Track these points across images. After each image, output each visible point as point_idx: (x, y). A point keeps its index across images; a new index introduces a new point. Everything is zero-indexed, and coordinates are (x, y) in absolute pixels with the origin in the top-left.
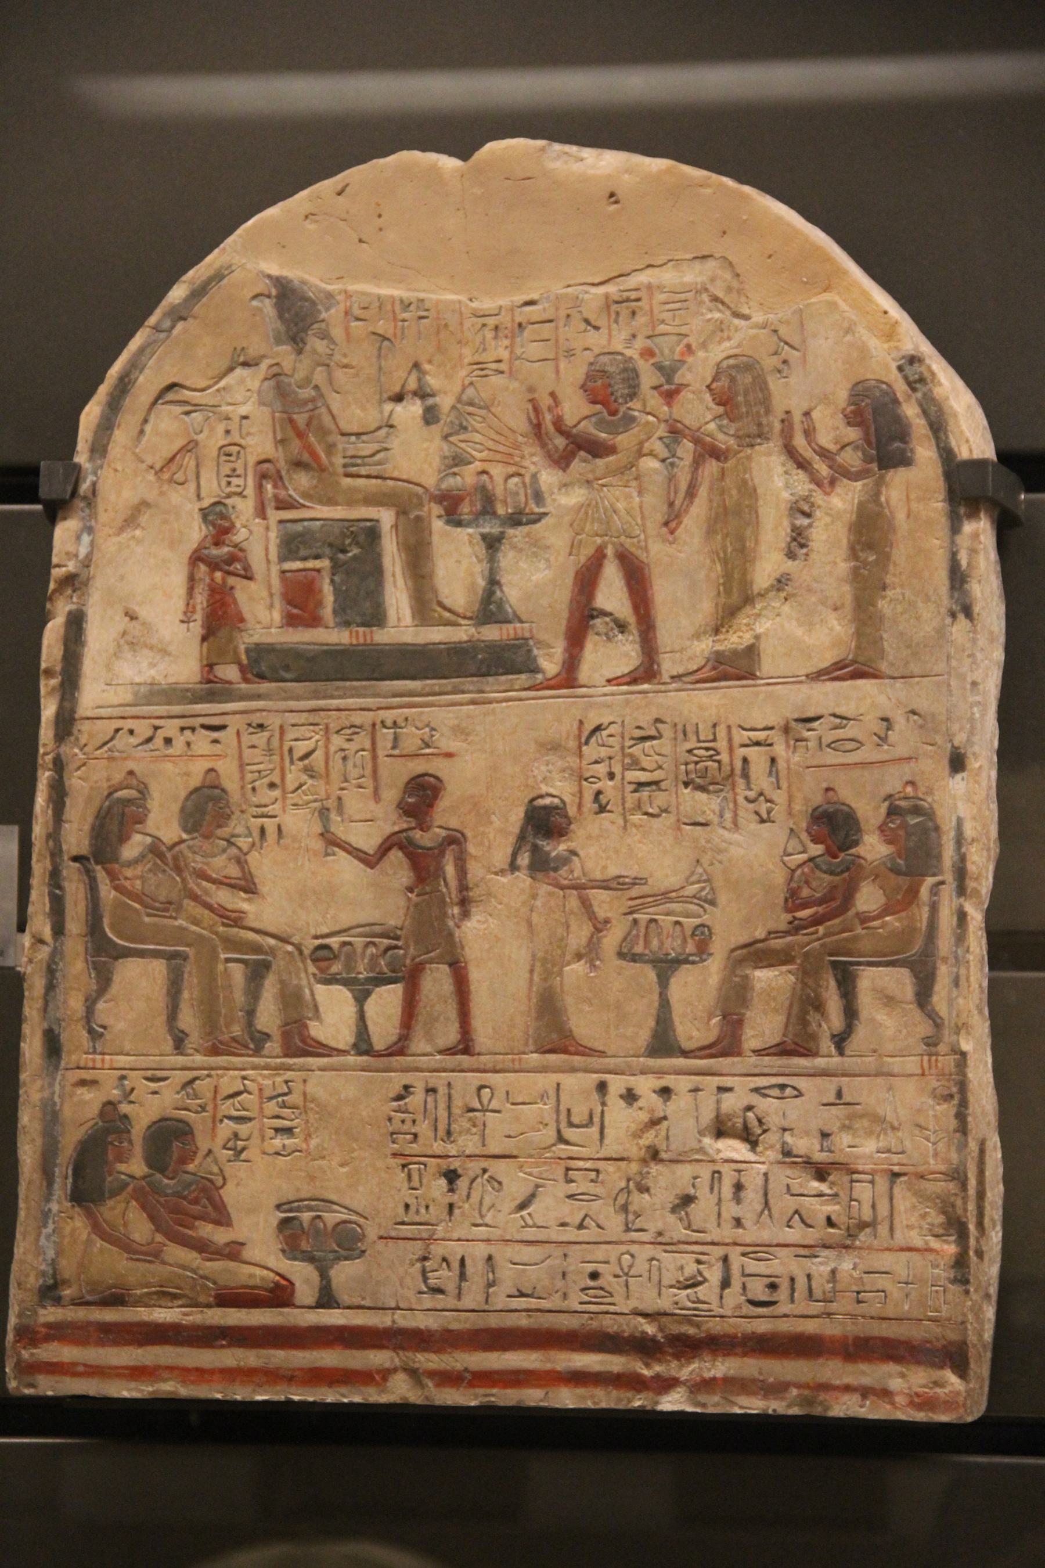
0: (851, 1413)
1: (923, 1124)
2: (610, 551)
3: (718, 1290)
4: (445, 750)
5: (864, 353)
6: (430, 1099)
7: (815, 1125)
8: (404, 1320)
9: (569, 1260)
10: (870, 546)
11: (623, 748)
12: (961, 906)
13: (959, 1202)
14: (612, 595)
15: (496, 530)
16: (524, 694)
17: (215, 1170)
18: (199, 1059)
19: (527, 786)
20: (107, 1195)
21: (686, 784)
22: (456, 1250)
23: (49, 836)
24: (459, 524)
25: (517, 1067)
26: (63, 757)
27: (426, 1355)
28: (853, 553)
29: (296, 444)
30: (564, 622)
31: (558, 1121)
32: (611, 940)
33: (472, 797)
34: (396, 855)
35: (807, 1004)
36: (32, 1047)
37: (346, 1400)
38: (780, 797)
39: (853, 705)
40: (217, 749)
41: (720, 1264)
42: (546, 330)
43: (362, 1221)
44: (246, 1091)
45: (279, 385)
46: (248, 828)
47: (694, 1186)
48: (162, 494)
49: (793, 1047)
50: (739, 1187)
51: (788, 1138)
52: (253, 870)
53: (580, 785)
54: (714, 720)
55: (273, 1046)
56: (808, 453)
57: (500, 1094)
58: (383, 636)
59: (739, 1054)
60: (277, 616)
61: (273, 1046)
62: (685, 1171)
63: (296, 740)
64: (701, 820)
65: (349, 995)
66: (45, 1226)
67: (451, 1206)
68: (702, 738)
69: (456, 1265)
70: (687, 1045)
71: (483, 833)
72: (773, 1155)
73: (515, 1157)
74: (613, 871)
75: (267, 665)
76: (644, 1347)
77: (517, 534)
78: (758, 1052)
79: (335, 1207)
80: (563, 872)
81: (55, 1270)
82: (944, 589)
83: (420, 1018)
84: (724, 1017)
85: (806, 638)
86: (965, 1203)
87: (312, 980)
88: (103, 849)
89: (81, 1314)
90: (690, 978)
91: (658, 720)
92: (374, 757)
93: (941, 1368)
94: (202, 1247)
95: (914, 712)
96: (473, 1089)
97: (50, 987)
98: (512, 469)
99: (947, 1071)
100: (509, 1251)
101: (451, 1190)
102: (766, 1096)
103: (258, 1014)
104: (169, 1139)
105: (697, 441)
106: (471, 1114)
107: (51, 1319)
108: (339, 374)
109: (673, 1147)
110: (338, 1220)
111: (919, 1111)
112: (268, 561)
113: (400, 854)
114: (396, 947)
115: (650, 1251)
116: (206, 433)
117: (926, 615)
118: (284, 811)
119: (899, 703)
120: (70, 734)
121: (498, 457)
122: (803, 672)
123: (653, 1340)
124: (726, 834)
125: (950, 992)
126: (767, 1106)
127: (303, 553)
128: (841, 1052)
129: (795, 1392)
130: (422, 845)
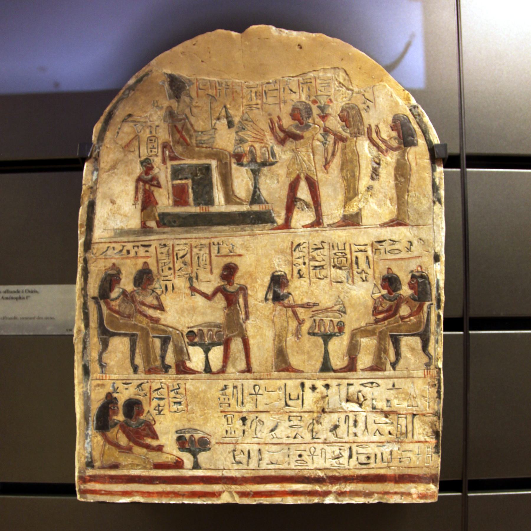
0: (397, 502)
1: (425, 395)
2: (302, 176)
3: (347, 460)
4: (238, 253)
5: (397, 104)
6: (235, 390)
7: (385, 397)
8: (226, 474)
9: (291, 450)
10: (402, 175)
11: (309, 253)
12: (439, 313)
13: (437, 424)
14: (303, 193)
15: (256, 168)
16: (270, 232)
17: (151, 418)
18: (143, 376)
19: (271, 267)
20: (109, 427)
21: (334, 267)
25: (269, 377)
26: (87, 258)
28: (396, 179)
29: (178, 136)
30: (285, 204)
31: (285, 398)
32: (305, 328)
33: (249, 272)
34: (219, 295)
35: (381, 351)
36: (78, 372)
37: (205, 503)
38: (370, 272)
39: (397, 236)
41: (348, 450)
42: (275, 93)
43: (209, 437)
44: (162, 388)
45: (171, 114)
46: (160, 285)
47: (338, 421)
48: (125, 155)
49: (376, 368)
50: (356, 421)
51: (374, 402)
52: (163, 302)
53: (292, 267)
54: (344, 241)
55: (173, 371)
56: (378, 141)
57: (263, 388)
59: (356, 371)
60: (171, 202)
61: (173, 371)
62: (335, 416)
63: (179, 250)
64: (340, 280)
65: (202, 350)
66: (87, 439)
67: (244, 432)
68: (340, 248)
69: (246, 453)
70: (335, 368)
71: (254, 286)
72: (369, 409)
74: (306, 300)
75: (166, 221)
76: (318, 480)
77: (265, 169)
78: (363, 370)
79: (199, 432)
80: (286, 301)
82: (431, 193)
83: (230, 359)
84: (350, 357)
85: (379, 210)
86: (439, 424)
87: (187, 344)
88: (104, 292)
89: (102, 472)
90: (336, 342)
91: (323, 242)
92: (210, 256)
93: (429, 483)
94: (148, 447)
95: (420, 239)
97: (85, 348)
98: (263, 145)
99: (434, 376)
100: (267, 447)
101: (244, 425)
102: (365, 386)
103: (166, 358)
104: (133, 407)
105: (335, 135)
106: (251, 396)
107: (91, 474)
108: (195, 110)
109: (330, 407)
110: (200, 437)
111: (423, 391)
112: (167, 181)
113: (221, 295)
114: (220, 331)
115: (322, 446)
116: (142, 132)
117: (424, 202)
118: (175, 278)
119: (415, 236)
121: (257, 140)
122: (378, 223)
123: (322, 478)
124: (350, 286)
125: (435, 346)
126: (367, 391)
127: (180, 177)
128: (394, 369)
129: (376, 495)
130: (230, 291)
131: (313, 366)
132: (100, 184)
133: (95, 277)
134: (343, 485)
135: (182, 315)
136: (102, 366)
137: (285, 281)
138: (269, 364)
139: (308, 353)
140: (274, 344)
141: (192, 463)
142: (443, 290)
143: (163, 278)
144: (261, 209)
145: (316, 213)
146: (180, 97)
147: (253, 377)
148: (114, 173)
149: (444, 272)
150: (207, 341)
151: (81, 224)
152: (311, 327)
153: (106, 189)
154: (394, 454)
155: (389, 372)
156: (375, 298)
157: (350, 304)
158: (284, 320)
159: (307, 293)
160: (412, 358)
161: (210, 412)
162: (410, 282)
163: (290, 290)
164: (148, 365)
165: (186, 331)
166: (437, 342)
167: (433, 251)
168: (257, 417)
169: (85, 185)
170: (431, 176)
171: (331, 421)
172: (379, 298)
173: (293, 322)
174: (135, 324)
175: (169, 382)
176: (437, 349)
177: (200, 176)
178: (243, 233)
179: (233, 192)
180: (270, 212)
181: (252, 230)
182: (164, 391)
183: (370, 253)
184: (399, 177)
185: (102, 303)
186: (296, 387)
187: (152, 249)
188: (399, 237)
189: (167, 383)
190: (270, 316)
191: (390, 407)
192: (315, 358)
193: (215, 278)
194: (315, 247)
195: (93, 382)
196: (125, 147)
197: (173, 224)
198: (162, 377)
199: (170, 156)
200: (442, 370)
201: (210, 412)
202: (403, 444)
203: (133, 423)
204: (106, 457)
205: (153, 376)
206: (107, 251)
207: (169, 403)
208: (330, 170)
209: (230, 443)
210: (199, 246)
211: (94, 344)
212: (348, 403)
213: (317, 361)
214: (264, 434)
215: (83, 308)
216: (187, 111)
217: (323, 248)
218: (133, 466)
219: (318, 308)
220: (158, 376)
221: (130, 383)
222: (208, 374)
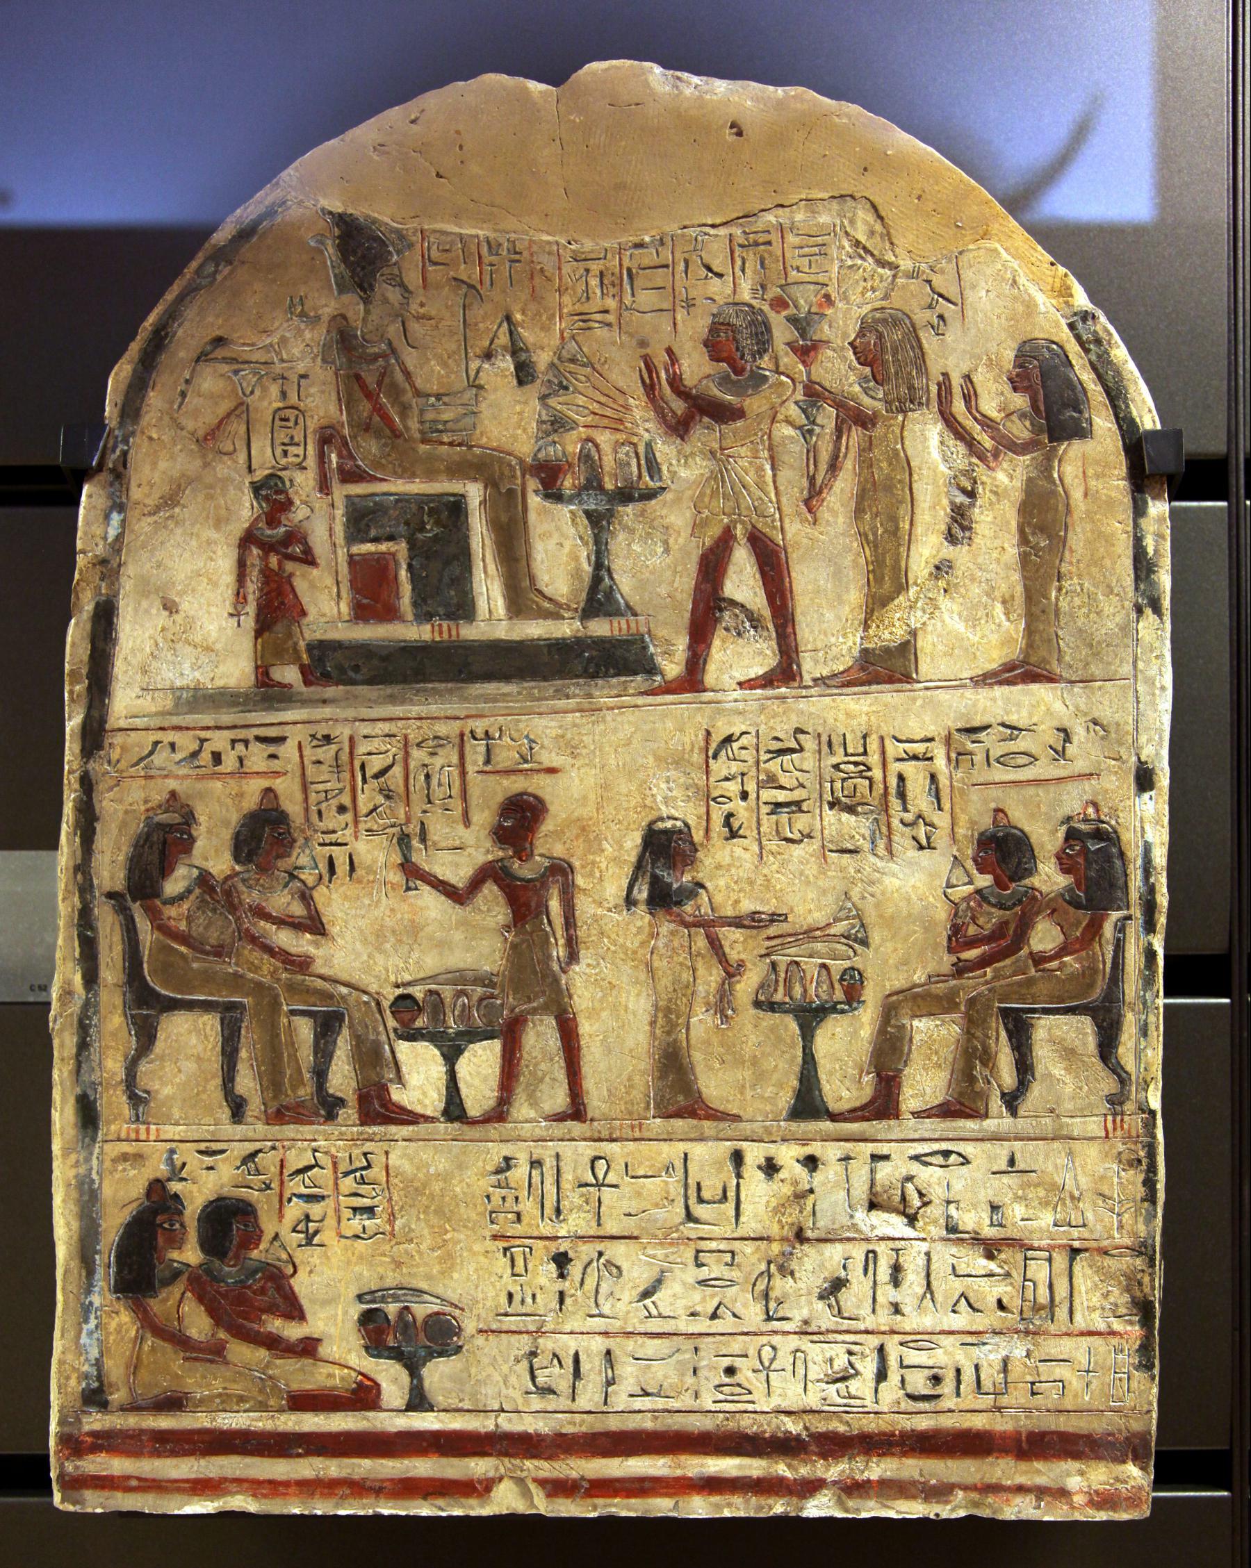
0: (1023, 1517)
1: (1107, 1192)
2: (739, 531)
3: (873, 1385)
4: (547, 763)
5: (1030, 306)
7: (985, 1195)
8: (508, 1424)
9: (701, 1353)
10: (1042, 529)
11: (758, 763)
12: (1150, 944)
13: (1146, 1279)
14: (743, 583)
15: (602, 508)
16: (640, 700)
17: (284, 1256)
18: (261, 1128)
21: (832, 805)
22: (570, 1344)
23: (77, 869)
24: (558, 498)
25: (637, 1135)
27: (536, 1462)
28: (1023, 540)
29: (365, 407)
30: (687, 615)
31: (686, 1197)
32: (746, 986)
34: (490, 890)
35: (972, 1057)
36: (63, 1116)
37: (444, 1514)
39: (1024, 713)
40: (276, 765)
41: (875, 1355)
42: (660, 277)
43: (457, 1313)
44: (317, 1165)
45: (344, 341)
46: (313, 858)
47: (844, 1267)
48: (206, 465)
50: (897, 1269)
52: (320, 907)
53: (708, 806)
54: (864, 729)
55: (349, 1113)
56: (969, 423)
58: (470, 632)
60: (344, 608)
61: (349, 1113)
62: (835, 1252)
65: (437, 1052)
66: (86, 1321)
67: (562, 1296)
68: (850, 751)
69: (568, 1362)
70: (833, 1106)
71: (593, 863)
72: (938, 1231)
73: (636, 1238)
74: (747, 906)
75: (332, 665)
76: (785, 1446)
77: (628, 512)
78: (917, 1115)
80: (688, 908)
81: (99, 1370)
82: (1129, 581)
84: (878, 1075)
87: (392, 1035)
89: (132, 1421)
92: (463, 773)
93: (1124, 1462)
94: (273, 1343)
96: (587, 1160)
97: (83, 1045)
98: (621, 437)
99: (1134, 1133)
100: (630, 1344)
101: (562, 1276)
104: (228, 1222)
105: (839, 405)
106: (584, 1189)
107: (97, 1426)
108: (415, 327)
109: (820, 1224)
110: (429, 1311)
111: (1102, 1178)
114: (492, 996)
115: (794, 1342)
116: (257, 393)
117: (1108, 610)
118: (356, 838)
120: (100, 747)
121: (606, 422)
123: (797, 1438)
124: (880, 864)
125: (1137, 1043)
126: (929, 1176)
127: (373, 533)
128: (1013, 1112)
129: (960, 1494)
130: (522, 876)
131: (768, 1099)
132: (129, 551)
133: (115, 831)
134: (859, 1463)
135: (379, 949)
136: (137, 1099)
137: (687, 847)
138: (637, 1095)
139: (755, 1061)
140: (653, 1034)
141: (407, 1390)
142: (1165, 874)
143: (321, 838)
144: (616, 632)
145: (779, 645)
146: (372, 287)
147: (588, 1135)
148: (172, 517)
149: (1166, 820)
150: (452, 1025)
151: (72, 671)
152: (762, 986)
153: (148, 566)
154: (1016, 1371)
155: (999, 1121)
156: (955, 898)
157: (881, 916)
158: (681, 964)
159: (751, 883)
160: (1068, 1079)
161: (462, 1237)
162: (1064, 851)
163: (700, 876)
164: (275, 1097)
165: (390, 994)
166: (1144, 1032)
167: (1134, 759)
168: (600, 1254)
169: (83, 552)
170: (1130, 529)
171: (822, 1266)
172: (966, 899)
173: (709, 969)
174: (235, 974)
175: (340, 1149)
176: (1144, 1053)
177: (431, 530)
178: (562, 703)
179: (532, 579)
180: (643, 641)
181: (590, 696)
182: (323, 1175)
183: (940, 763)
184: (1033, 534)
185: (137, 909)
186: (718, 1165)
187: (288, 750)
188: (1031, 715)
189: (333, 1150)
190: (641, 951)
191: (1001, 1225)
192: (775, 1076)
193: (478, 839)
194: (776, 745)
195: (107, 1147)
196: (205, 439)
197: (351, 674)
198: (317, 1132)
199: (340, 468)
200: (1159, 1116)
201: (462, 1237)
202: (1040, 1340)
203: (229, 1271)
204: (144, 1374)
205: (290, 1130)
206: (151, 753)
207: (337, 1211)
208: (824, 514)
209: (520, 1333)
210: (431, 743)
211: (114, 1035)
212: (874, 1213)
213: (780, 1085)
214: (622, 1305)
215: (79, 925)
216: (393, 330)
217: (801, 750)
218: (227, 1402)
219: (784, 928)
220: (307, 1130)
221: (222, 1152)
222: (457, 1125)
